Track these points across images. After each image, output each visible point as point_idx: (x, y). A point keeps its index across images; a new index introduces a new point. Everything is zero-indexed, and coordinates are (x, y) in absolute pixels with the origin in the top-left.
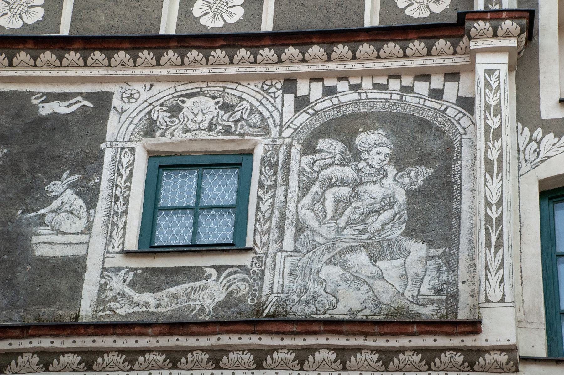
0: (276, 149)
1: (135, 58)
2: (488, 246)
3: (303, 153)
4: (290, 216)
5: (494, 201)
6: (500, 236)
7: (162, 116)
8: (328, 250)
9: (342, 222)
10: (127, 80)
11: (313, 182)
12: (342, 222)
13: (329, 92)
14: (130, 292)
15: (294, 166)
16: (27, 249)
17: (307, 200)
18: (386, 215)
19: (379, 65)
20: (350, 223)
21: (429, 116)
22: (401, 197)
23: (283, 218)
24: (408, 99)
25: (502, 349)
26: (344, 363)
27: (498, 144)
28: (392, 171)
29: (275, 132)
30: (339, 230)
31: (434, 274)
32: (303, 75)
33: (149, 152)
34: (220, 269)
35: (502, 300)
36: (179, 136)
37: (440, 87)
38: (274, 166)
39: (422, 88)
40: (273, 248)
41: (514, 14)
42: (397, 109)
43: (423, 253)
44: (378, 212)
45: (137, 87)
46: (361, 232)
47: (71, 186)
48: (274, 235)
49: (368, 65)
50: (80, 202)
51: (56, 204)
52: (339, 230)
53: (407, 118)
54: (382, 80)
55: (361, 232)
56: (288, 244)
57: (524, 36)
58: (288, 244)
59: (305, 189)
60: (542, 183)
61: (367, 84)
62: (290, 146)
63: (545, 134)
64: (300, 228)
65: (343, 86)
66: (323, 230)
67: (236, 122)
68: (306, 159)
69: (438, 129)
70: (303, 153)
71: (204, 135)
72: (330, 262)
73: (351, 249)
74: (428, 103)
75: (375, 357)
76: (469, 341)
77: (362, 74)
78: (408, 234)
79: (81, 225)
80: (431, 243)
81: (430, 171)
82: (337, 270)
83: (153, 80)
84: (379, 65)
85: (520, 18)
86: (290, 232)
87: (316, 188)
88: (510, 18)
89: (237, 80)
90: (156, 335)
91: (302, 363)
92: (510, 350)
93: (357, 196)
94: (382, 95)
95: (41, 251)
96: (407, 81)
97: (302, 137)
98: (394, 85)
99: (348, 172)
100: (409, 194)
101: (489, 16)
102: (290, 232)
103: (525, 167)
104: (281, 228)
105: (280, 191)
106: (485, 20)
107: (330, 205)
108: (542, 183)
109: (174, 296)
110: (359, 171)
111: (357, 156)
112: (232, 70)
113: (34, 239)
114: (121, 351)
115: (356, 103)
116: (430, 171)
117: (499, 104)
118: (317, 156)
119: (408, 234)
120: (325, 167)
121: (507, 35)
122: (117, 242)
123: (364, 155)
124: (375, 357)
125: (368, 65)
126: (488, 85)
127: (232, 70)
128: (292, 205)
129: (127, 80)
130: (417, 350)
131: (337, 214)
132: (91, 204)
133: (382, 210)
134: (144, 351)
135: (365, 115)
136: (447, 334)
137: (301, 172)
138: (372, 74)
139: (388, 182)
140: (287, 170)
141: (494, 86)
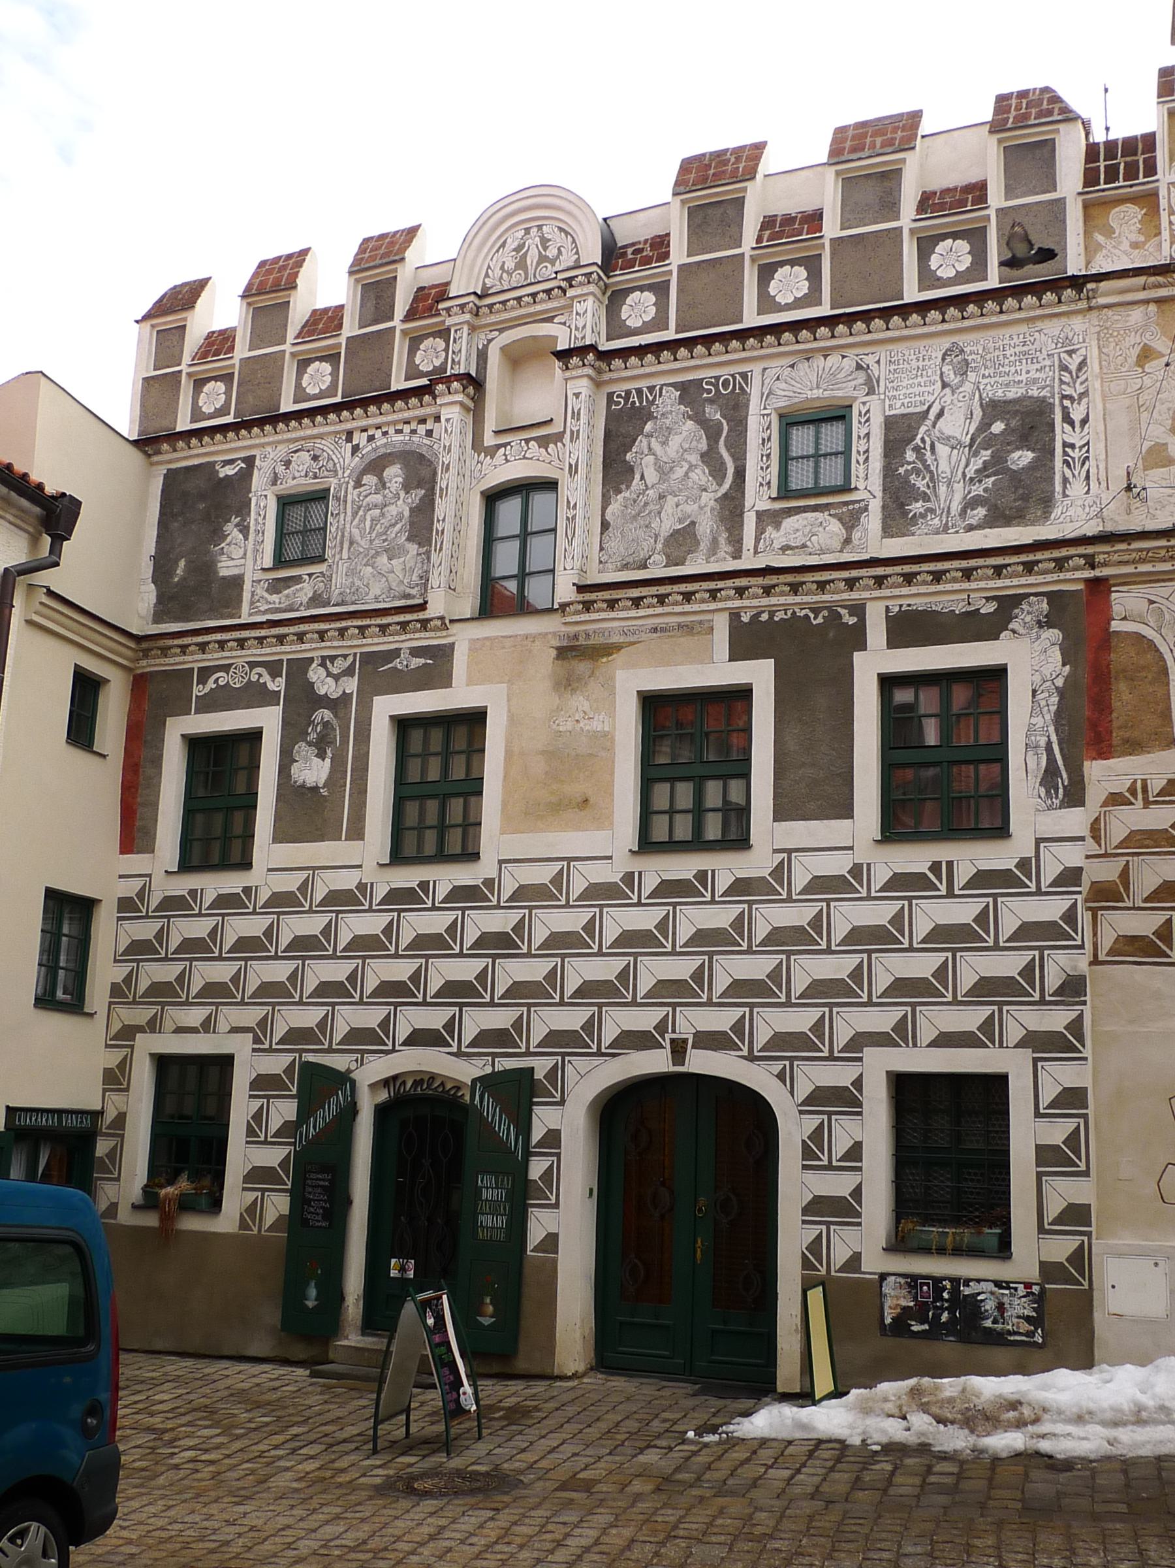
0: (340, 486)
1: (263, 430)
2: (435, 550)
3: (355, 488)
4: (346, 534)
5: (441, 518)
6: (442, 542)
7: (281, 469)
8: (366, 556)
9: (374, 535)
10: (263, 445)
11: (359, 508)
12: (374, 535)
13: (371, 438)
14: (266, 595)
15: (349, 497)
16: (216, 572)
17: (356, 522)
18: (398, 526)
19: (395, 417)
20: (379, 535)
21: (424, 451)
22: (407, 513)
23: (343, 536)
24: (414, 439)
25: (438, 618)
26: (363, 634)
27: (447, 475)
28: (402, 493)
29: (340, 473)
30: (371, 541)
31: (421, 565)
32: (356, 428)
33: (277, 495)
34: (310, 575)
35: (439, 587)
36: (291, 483)
37: (431, 428)
38: (338, 499)
39: (422, 429)
40: (338, 557)
41: (459, 377)
42: (407, 448)
43: (415, 552)
44: (394, 525)
45: (269, 449)
46: (384, 541)
47: (236, 526)
48: (338, 549)
49: (390, 418)
50: (241, 536)
51: (229, 538)
52: (371, 541)
53: (413, 453)
54: (399, 427)
55: (384, 541)
56: (345, 555)
57: (471, 390)
58: (345, 555)
59: (355, 514)
60: (482, 493)
61: (392, 431)
62: (348, 483)
63: (486, 456)
64: (351, 543)
65: (378, 434)
66: (363, 543)
67: (320, 469)
68: (356, 492)
69: (429, 460)
70: (355, 488)
71: (303, 481)
72: (366, 565)
73: (377, 553)
74: (424, 441)
75: (378, 629)
76: (421, 615)
77: (388, 424)
78: (409, 539)
79: (241, 551)
80: (420, 545)
81: (423, 492)
82: (370, 569)
83: (276, 444)
84: (395, 417)
85: (462, 379)
86: (346, 546)
87: (361, 513)
88: (457, 381)
89: (320, 436)
90: (269, 628)
91: (343, 637)
92: (442, 618)
93: (383, 515)
94: (400, 437)
95: (223, 573)
96: (413, 425)
97: (355, 475)
98: (407, 429)
99: (377, 498)
100: (410, 509)
101: (444, 380)
102: (346, 546)
103: (474, 482)
104: (342, 543)
105: (342, 516)
106: (442, 383)
107: (368, 523)
108: (482, 493)
109: (287, 596)
110: (385, 497)
111: (384, 486)
112: (316, 431)
113: (219, 565)
114: (255, 638)
115: (385, 445)
116: (423, 492)
117: (450, 445)
118: (362, 489)
119: (409, 539)
120: (366, 496)
121: (456, 392)
122: (259, 562)
123: (388, 485)
124: (378, 629)
125: (390, 418)
126: (446, 430)
127: (316, 431)
128: (348, 526)
129: (263, 445)
130: (398, 623)
131: (372, 529)
132: (246, 538)
133: (396, 523)
134: (265, 638)
135: (390, 454)
136: (410, 612)
137: (353, 502)
138: (395, 423)
139: (400, 502)
140: (345, 501)
141: (449, 430)
